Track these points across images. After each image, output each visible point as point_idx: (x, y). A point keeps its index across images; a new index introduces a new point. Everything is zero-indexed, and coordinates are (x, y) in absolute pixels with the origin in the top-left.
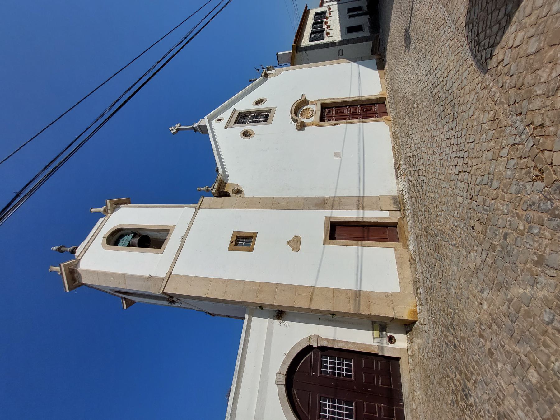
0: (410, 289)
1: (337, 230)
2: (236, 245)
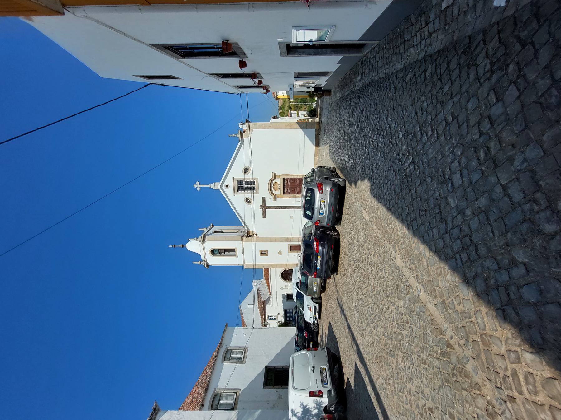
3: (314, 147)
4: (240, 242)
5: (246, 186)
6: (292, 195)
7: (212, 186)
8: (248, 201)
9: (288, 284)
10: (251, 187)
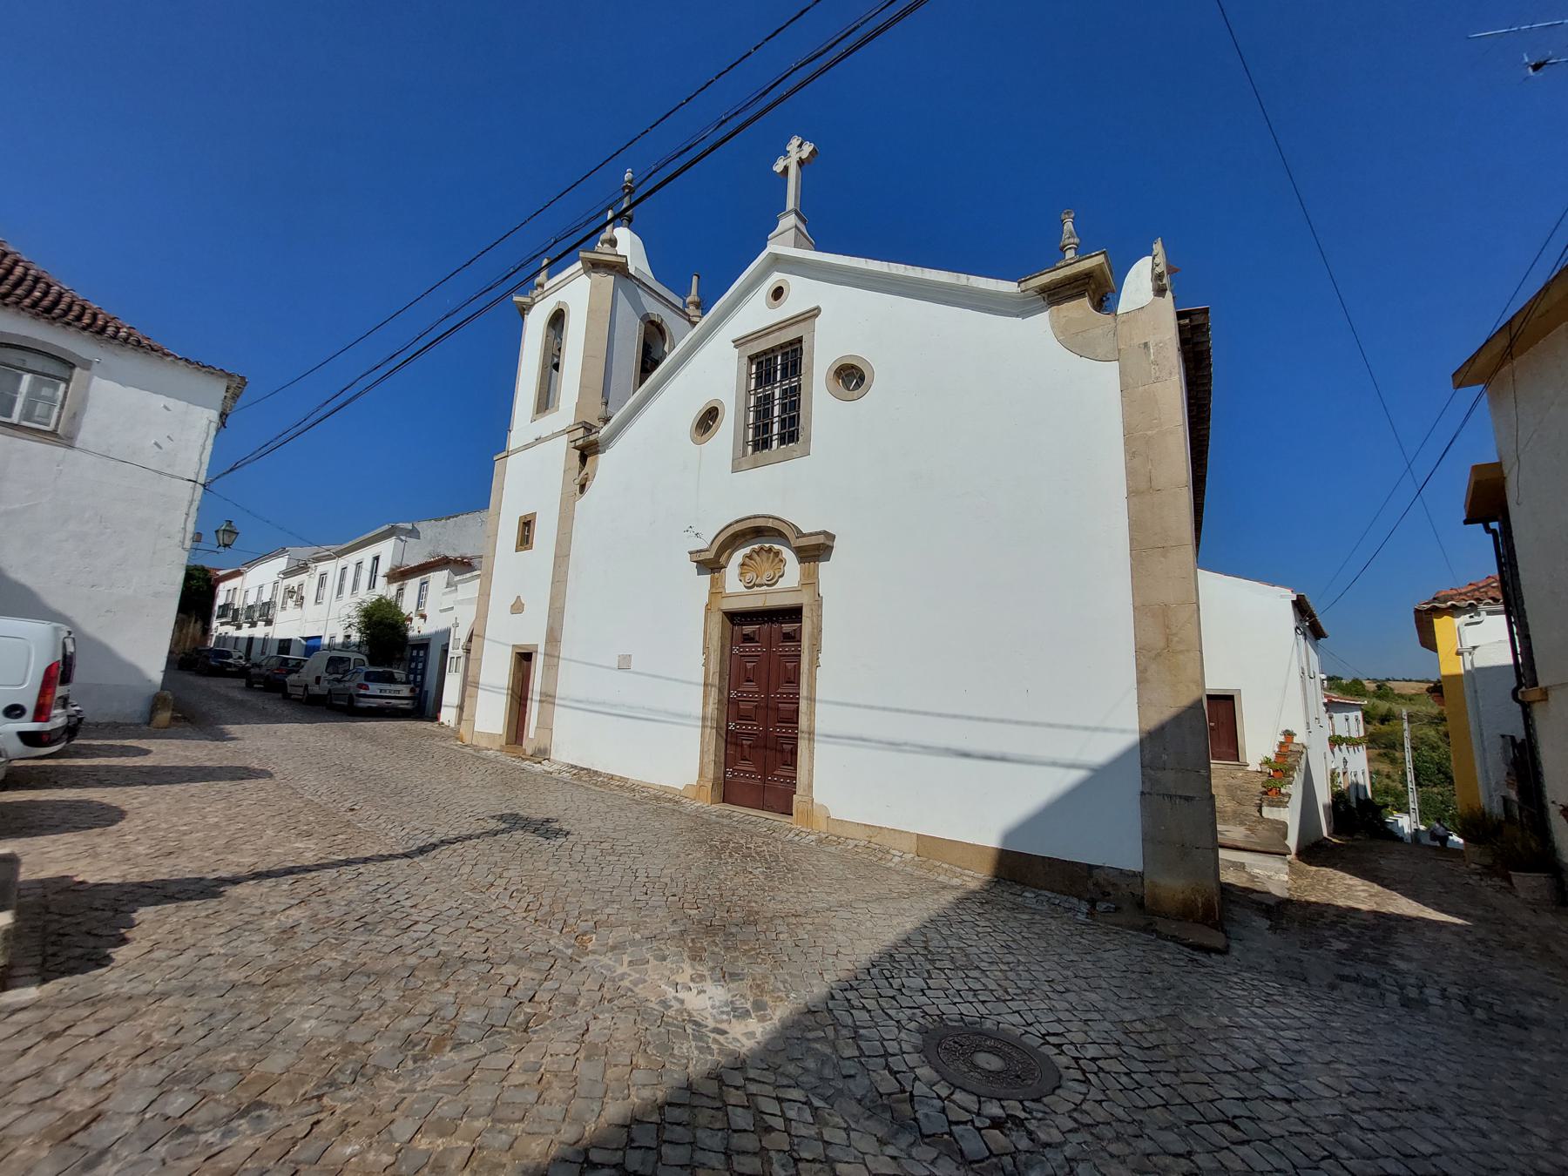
1: (524, 658)
5: (777, 393)
6: (714, 666)
7: (788, 222)
8: (708, 419)
10: (767, 428)
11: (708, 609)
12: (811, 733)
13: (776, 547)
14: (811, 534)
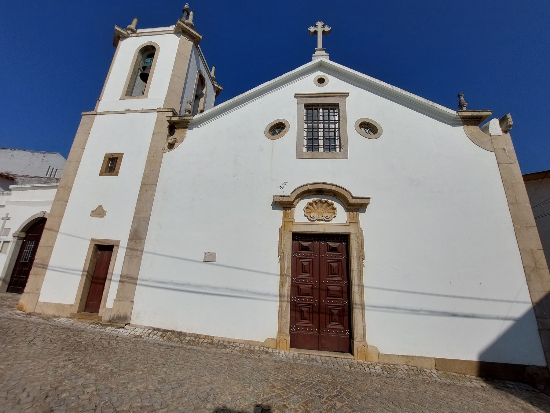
0: (38, 310)
1: (103, 251)
2: (110, 159)
3: (472, 355)
4: (160, 105)
6: (288, 263)
8: (278, 128)
9: (10, 238)
11: (282, 230)
12: (362, 305)
13: (330, 201)
14: (358, 198)
